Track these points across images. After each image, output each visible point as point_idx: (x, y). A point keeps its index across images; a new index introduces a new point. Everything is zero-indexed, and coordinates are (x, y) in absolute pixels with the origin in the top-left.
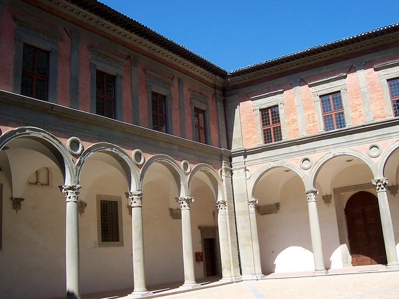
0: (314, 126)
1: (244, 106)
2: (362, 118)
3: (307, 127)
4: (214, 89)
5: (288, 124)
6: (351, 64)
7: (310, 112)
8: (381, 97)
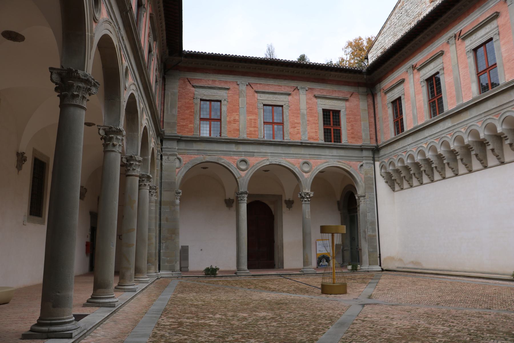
0: (255, 131)
1: (183, 91)
2: (298, 135)
3: (248, 130)
5: (229, 122)
7: (253, 117)
8: (317, 122)
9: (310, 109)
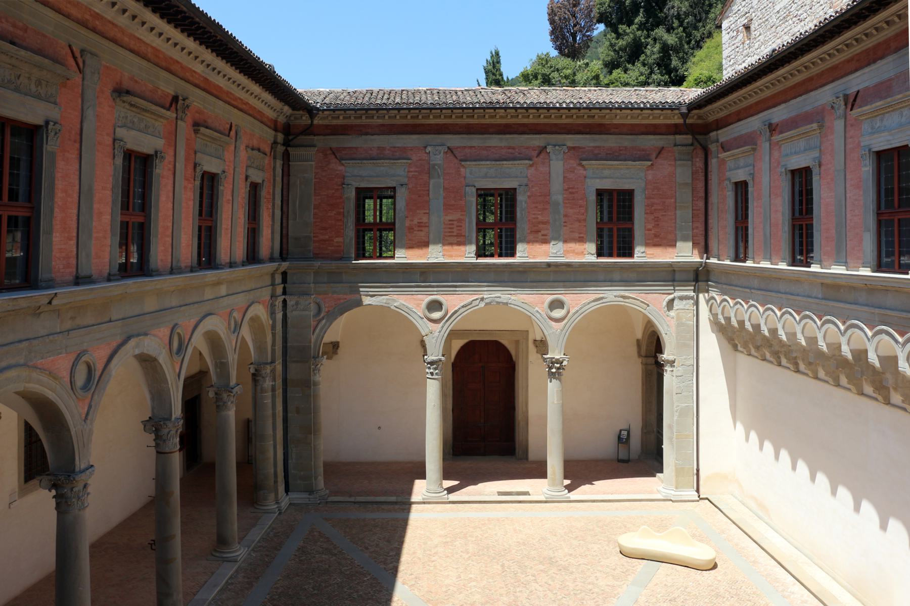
4: (273, 133)
5: (411, 229)
6: (543, 145)
8: (583, 217)
9: (572, 191)
